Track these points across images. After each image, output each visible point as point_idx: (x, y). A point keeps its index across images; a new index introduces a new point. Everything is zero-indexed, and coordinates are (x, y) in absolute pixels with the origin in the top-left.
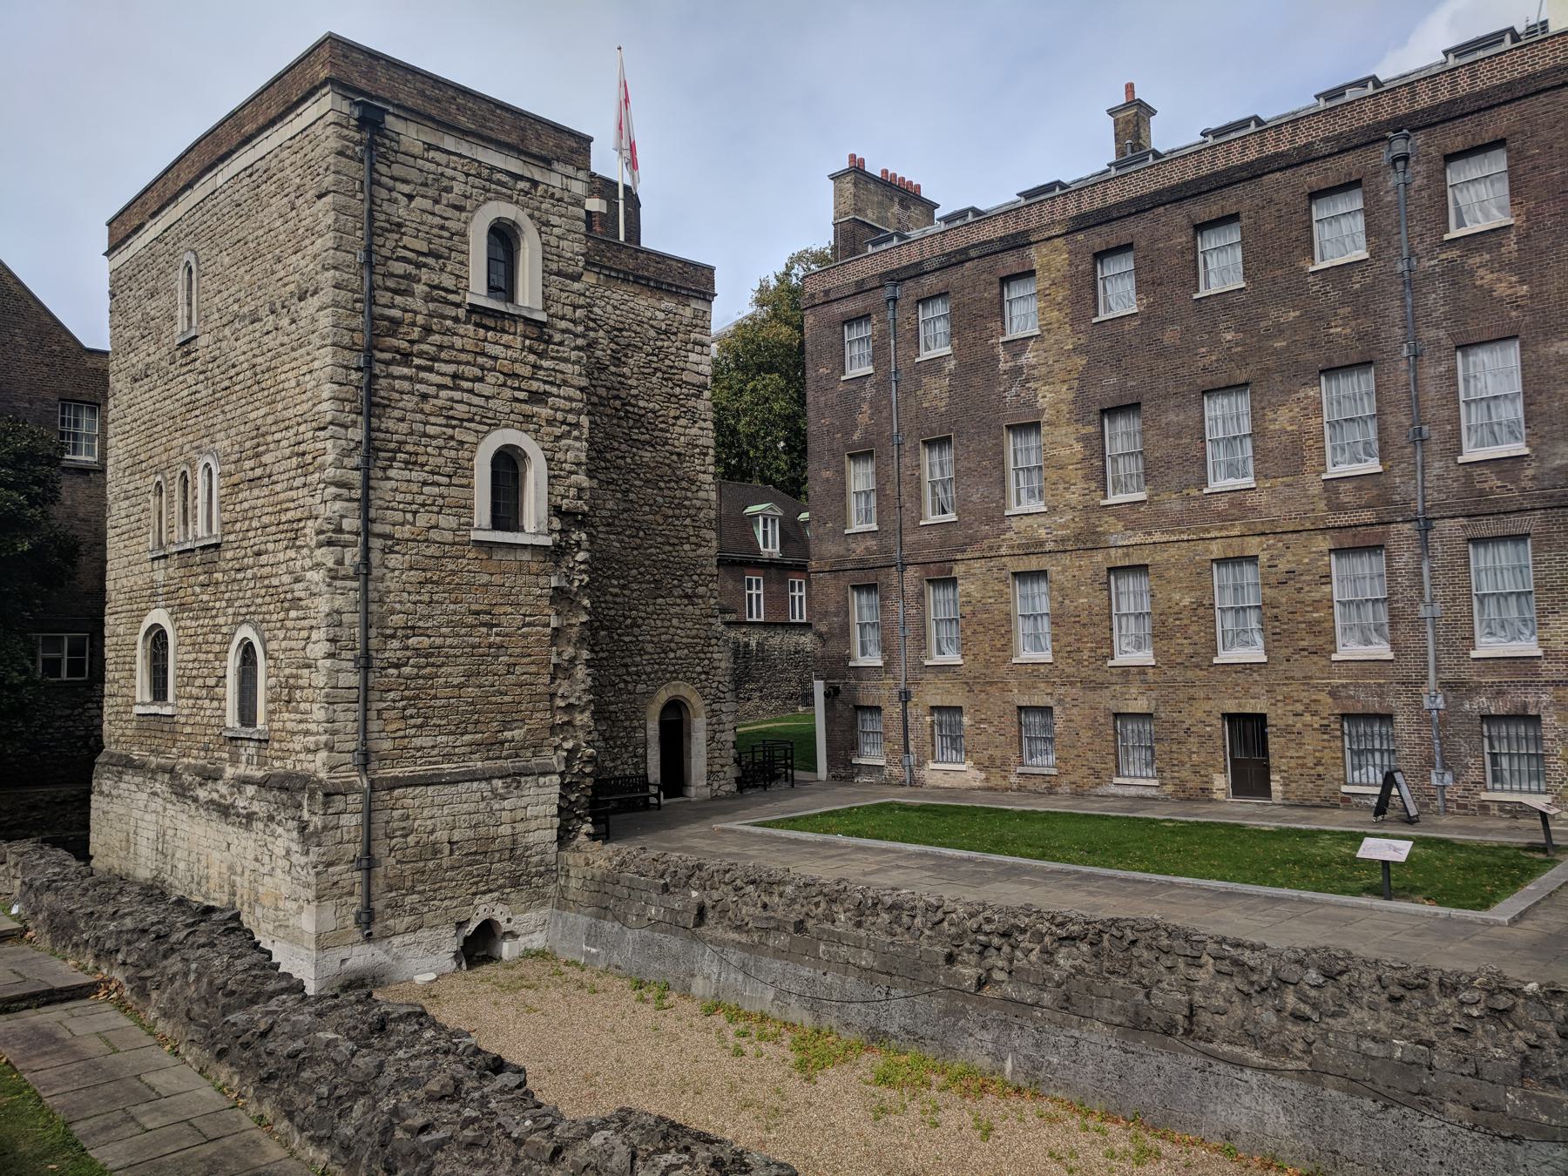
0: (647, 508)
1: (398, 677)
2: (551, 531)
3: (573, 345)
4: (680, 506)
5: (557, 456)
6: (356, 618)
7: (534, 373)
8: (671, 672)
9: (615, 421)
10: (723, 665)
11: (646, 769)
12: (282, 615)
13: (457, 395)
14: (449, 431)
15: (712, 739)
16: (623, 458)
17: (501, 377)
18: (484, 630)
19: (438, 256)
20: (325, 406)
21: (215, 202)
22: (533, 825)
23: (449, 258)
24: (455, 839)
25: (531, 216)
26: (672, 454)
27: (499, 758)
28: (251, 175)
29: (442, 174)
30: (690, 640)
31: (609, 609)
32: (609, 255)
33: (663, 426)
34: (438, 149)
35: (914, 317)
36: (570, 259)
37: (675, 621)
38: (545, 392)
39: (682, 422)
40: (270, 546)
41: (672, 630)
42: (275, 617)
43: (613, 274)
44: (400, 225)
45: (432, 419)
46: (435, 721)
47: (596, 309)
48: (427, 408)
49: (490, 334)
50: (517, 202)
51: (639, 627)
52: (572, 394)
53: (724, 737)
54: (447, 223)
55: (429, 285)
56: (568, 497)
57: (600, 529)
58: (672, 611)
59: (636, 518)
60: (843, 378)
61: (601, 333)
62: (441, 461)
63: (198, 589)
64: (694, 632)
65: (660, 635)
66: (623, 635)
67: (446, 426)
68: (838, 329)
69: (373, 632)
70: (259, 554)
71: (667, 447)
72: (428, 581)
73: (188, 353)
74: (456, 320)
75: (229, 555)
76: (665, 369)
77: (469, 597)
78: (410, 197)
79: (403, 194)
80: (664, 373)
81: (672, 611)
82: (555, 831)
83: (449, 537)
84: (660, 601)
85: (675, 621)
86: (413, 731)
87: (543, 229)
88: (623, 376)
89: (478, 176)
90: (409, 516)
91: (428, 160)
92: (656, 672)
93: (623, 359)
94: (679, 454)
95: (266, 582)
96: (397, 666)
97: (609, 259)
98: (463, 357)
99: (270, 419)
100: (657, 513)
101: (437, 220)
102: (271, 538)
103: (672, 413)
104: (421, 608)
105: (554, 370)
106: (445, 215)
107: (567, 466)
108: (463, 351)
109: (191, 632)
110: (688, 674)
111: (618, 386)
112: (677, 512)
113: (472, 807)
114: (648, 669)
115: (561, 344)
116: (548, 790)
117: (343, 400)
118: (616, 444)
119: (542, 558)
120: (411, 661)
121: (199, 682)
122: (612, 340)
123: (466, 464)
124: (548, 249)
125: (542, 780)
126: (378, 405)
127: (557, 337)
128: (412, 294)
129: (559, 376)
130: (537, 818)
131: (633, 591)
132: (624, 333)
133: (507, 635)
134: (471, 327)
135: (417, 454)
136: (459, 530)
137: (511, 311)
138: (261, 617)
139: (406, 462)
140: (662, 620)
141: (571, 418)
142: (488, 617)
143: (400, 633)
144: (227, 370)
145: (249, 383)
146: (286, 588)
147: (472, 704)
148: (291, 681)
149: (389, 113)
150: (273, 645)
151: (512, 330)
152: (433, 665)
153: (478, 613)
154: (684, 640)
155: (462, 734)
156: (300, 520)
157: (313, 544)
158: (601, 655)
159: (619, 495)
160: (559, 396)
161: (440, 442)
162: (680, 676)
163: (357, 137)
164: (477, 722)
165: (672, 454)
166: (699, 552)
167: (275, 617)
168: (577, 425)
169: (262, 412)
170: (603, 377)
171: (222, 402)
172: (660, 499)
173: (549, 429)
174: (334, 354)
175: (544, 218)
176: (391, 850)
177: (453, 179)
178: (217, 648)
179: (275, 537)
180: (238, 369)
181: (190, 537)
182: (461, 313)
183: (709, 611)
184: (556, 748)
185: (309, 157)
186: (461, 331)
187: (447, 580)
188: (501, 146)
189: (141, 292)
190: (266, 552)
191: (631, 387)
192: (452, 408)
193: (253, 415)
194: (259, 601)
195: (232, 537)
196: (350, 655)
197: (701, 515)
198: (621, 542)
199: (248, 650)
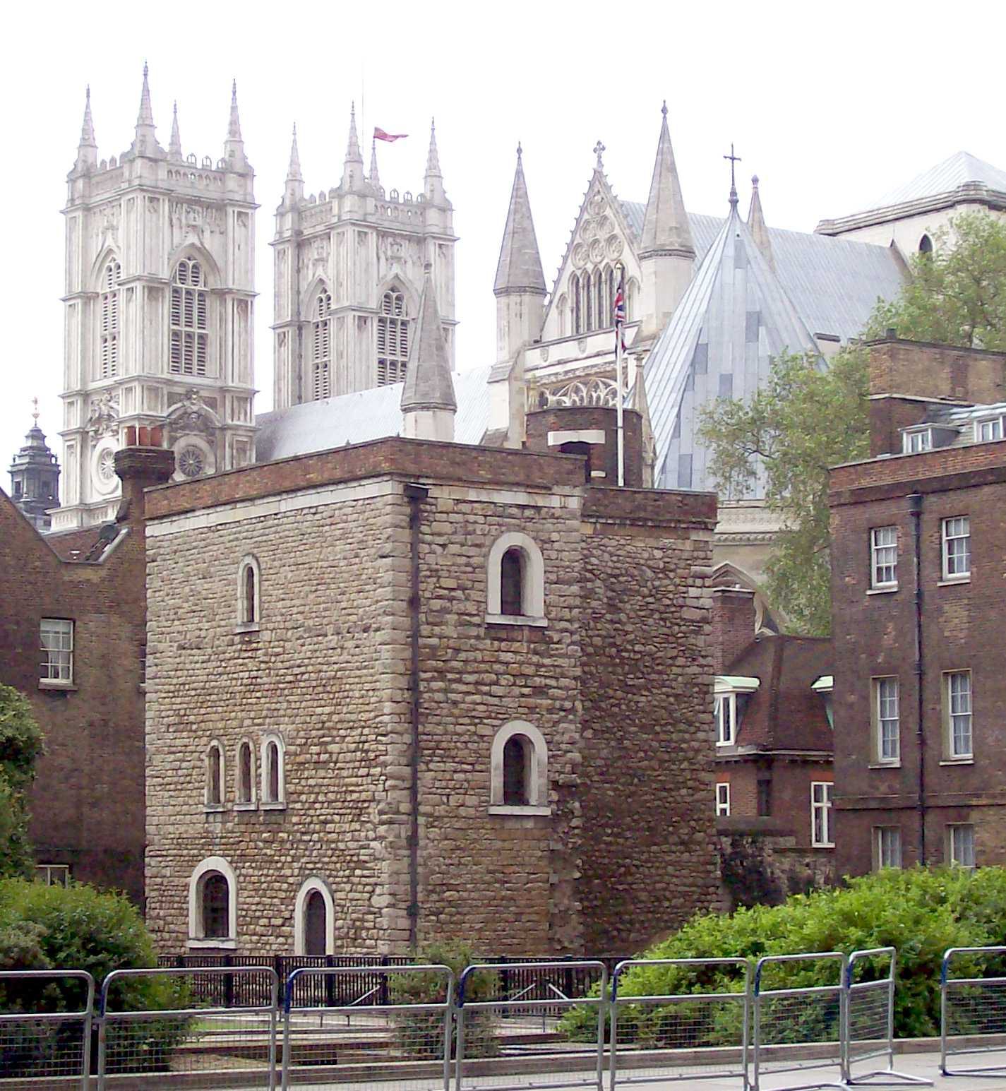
1: (438, 921)
3: (569, 641)
5: (556, 738)
6: (407, 878)
7: (537, 671)
9: (610, 669)
12: (347, 872)
14: (472, 728)
16: (618, 705)
17: (511, 678)
19: (464, 589)
20: (386, 719)
21: (276, 521)
23: (472, 588)
25: (534, 539)
26: (668, 696)
28: (314, 514)
29: (467, 521)
30: (687, 889)
32: (606, 502)
33: (660, 668)
34: (465, 502)
35: (937, 535)
36: (568, 567)
37: (670, 869)
39: (681, 661)
40: (337, 818)
42: (341, 873)
44: (437, 571)
45: (461, 721)
47: (594, 560)
48: (456, 712)
49: (503, 644)
50: (523, 529)
51: (631, 874)
55: (458, 614)
56: (562, 773)
57: (596, 778)
58: (668, 858)
59: (631, 764)
60: (869, 592)
62: (467, 751)
63: (261, 844)
65: (656, 882)
68: (865, 536)
69: (420, 888)
70: (325, 822)
72: (458, 848)
73: (250, 642)
74: (478, 637)
75: (295, 819)
76: (662, 608)
78: (444, 546)
80: (661, 613)
81: (668, 858)
83: (472, 811)
84: (654, 848)
87: (546, 546)
90: (445, 799)
92: (648, 920)
93: (620, 605)
94: (676, 696)
95: (333, 846)
96: (437, 914)
97: (606, 506)
99: (335, 718)
102: (336, 811)
105: (553, 666)
107: (563, 746)
108: (483, 662)
109: (254, 879)
111: (613, 633)
112: (673, 755)
117: (399, 714)
118: (611, 692)
120: (447, 910)
121: (263, 921)
123: (483, 752)
126: (422, 714)
127: (556, 638)
128: (446, 624)
129: (558, 670)
132: (622, 579)
134: (488, 642)
138: (328, 872)
139: (441, 756)
140: (658, 868)
141: (568, 705)
143: (438, 889)
144: (291, 667)
145: (314, 683)
146: (352, 852)
148: (358, 923)
150: (339, 895)
154: (680, 889)
156: (364, 801)
157: (376, 821)
158: (595, 903)
159: (613, 743)
161: (466, 738)
163: (408, 510)
166: (696, 797)
167: (341, 873)
168: (572, 710)
169: (327, 710)
171: (286, 692)
172: (655, 744)
174: (394, 679)
175: (545, 536)
177: (476, 522)
178: (283, 895)
179: (341, 811)
180: (303, 669)
181: (253, 799)
182: (482, 631)
185: (371, 521)
186: (481, 647)
189: (189, 569)
190: (332, 822)
191: (627, 633)
193: (319, 710)
194: (326, 859)
195: (298, 806)
196: (403, 905)
197: (700, 757)
198: (615, 790)
199: (315, 899)
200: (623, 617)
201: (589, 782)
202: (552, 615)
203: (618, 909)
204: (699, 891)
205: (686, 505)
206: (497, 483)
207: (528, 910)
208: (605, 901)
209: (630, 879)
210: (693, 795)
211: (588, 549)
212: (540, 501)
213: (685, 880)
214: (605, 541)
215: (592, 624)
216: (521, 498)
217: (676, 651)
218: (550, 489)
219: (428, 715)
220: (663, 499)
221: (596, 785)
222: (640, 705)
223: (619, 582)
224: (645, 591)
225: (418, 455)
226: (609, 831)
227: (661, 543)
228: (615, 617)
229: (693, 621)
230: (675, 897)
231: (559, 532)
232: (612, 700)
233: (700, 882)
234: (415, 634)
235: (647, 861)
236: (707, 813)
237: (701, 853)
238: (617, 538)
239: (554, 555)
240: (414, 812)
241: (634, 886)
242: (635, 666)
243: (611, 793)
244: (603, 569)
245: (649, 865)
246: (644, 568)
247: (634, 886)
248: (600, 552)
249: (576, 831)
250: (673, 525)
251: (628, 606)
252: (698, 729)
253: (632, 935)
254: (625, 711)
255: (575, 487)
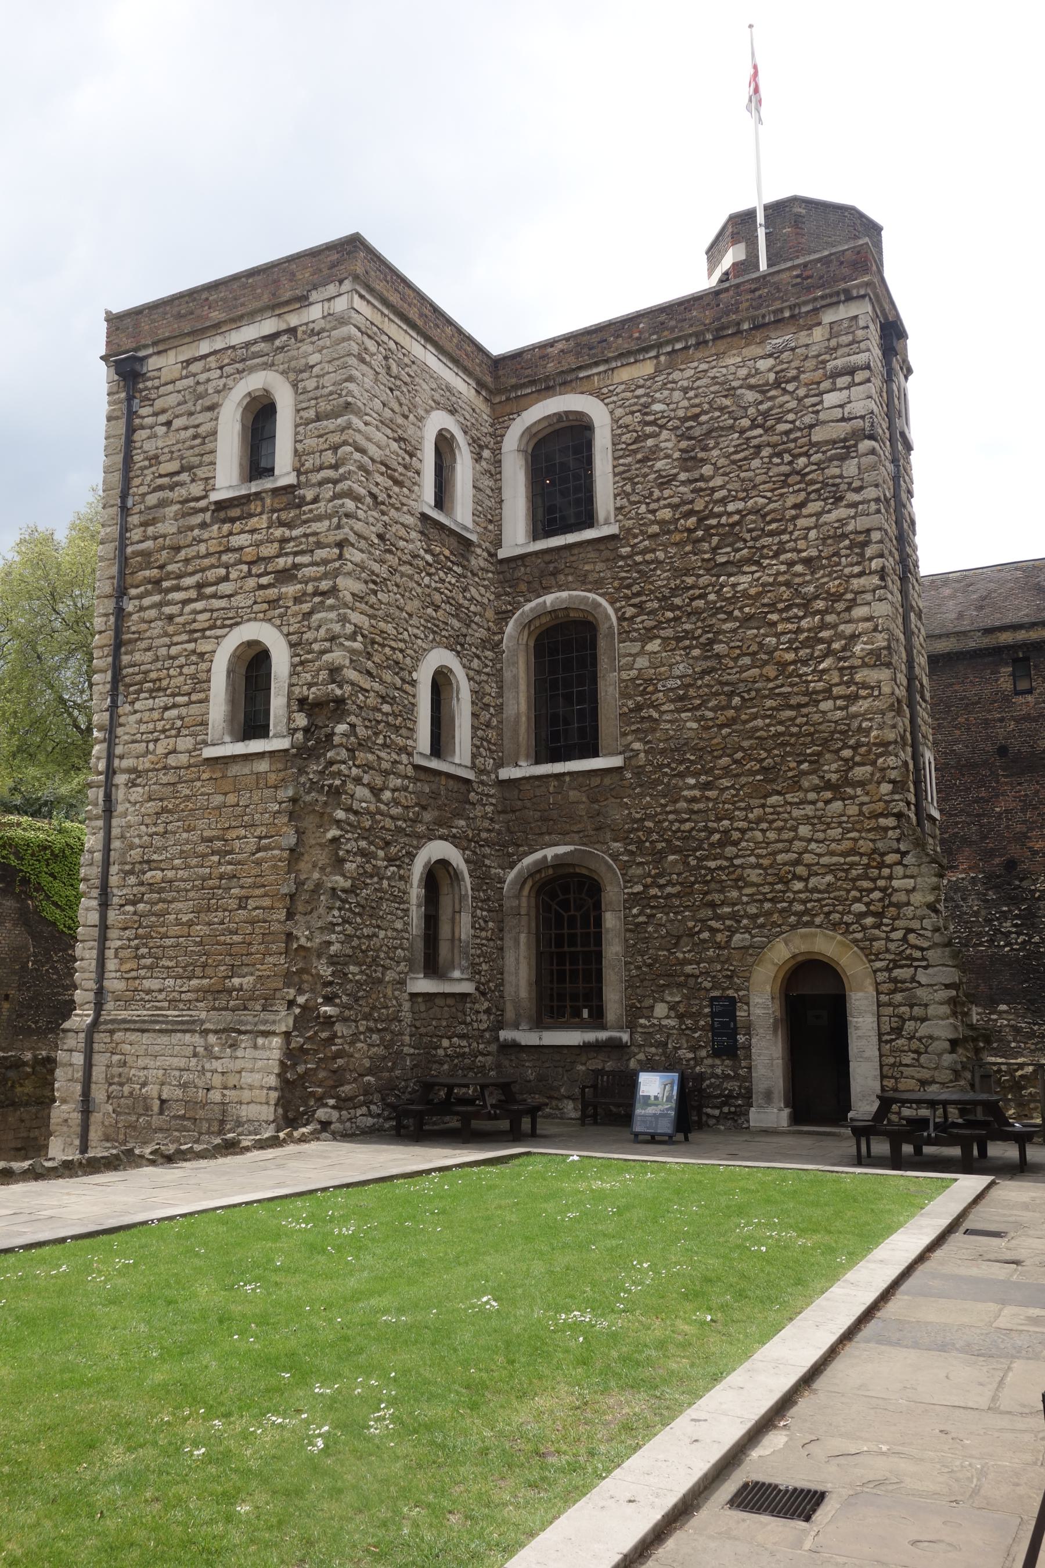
0: (747, 660)
1: (135, 913)
2: (293, 732)
4: (813, 641)
7: (282, 548)
8: (800, 914)
9: (688, 548)
10: (917, 898)
11: (750, 1068)
13: (199, 605)
14: (191, 646)
15: (898, 1031)
17: (245, 568)
18: (216, 858)
22: (246, 1095)
23: (200, 465)
24: (164, 1097)
27: (226, 1009)
29: (198, 383)
30: (835, 859)
31: (683, 821)
32: (673, 323)
33: (774, 526)
36: (331, 393)
37: (804, 830)
38: (296, 566)
39: (814, 507)
41: (798, 845)
43: (678, 346)
44: (156, 457)
45: (175, 639)
46: (165, 962)
47: (657, 407)
48: (171, 629)
50: (273, 365)
51: (735, 844)
52: (324, 556)
53: (924, 1030)
54: (200, 430)
55: (179, 502)
56: (316, 684)
57: (665, 708)
58: (796, 813)
59: (726, 678)
61: (665, 435)
62: (182, 678)
64: (846, 845)
65: (774, 854)
66: (706, 858)
67: (189, 641)
69: (114, 869)
71: (782, 557)
72: (164, 810)
74: (203, 525)
76: (776, 438)
77: (201, 824)
79: (162, 425)
81: (796, 813)
82: (272, 1109)
83: (184, 759)
84: (774, 799)
85: (804, 830)
86: (142, 972)
88: (702, 478)
89: (234, 361)
90: (151, 746)
91: (187, 377)
92: (768, 914)
94: (807, 562)
96: (134, 903)
98: (206, 562)
100: (766, 663)
101: (191, 432)
103: (791, 500)
104: (158, 841)
105: (306, 535)
106: (197, 422)
107: (316, 647)
108: (208, 555)
110: (836, 917)
111: (691, 496)
112: (803, 653)
113: (182, 1063)
114: (752, 910)
115: (316, 500)
116: (267, 1054)
118: (690, 580)
119: (280, 766)
122: (682, 437)
123: (203, 676)
124: (302, 397)
125: (260, 1041)
126: (130, 641)
127: (309, 494)
129: (311, 539)
130: (251, 1087)
131: (723, 790)
132: (704, 418)
133: (239, 863)
135: (160, 680)
136: (195, 750)
137: (253, 490)
139: (151, 691)
140: (780, 830)
141: (325, 585)
142: (219, 844)
143: (138, 867)
147: (200, 944)
149: (150, 356)
151: (259, 510)
152: (164, 901)
153: (210, 840)
154: (825, 860)
155: (190, 978)
158: (669, 890)
160: (313, 564)
161: (182, 660)
162: (818, 920)
164: (204, 966)
165: (791, 564)
166: (853, 709)
170: (667, 493)
173: (296, 608)
176: (109, 1097)
177: (209, 380)
183: (879, 807)
184: (291, 1003)
186: (206, 536)
187: (182, 806)
188: (251, 316)
191: (713, 490)
192: (194, 621)
198: (698, 721)
200: (707, 470)
201: (656, 715)
202: (308, 465)
203: (709, 898)
204: (865, 860)
205: (808, 277)
206: (233, 320)
207: (260, 891)
208: (687, 889)
209: (730, 851)
210: (846, 708)
211: (647, 395)
212: (293, 320)
213: (833, 845)
214: (676, 375)
215: (657, 493)
216: (269, 326)
217: (803, 494)
218: (306, 298)
219: (136, 640)
220: (765, 286)
221: (666, 717)
222: (740, 588)
223: (700, 424)
224: (745, 423)
225: (137, 326)
226: (692, 781)
227: (769, 349)
228: (696, 474)
229: (834, 442)
230: (817, 874)
231: (320, 351)
232: (691, 592)
233: (865, 846)
234: (123, 542)
235: (759, 820)
236: (874, 733)
237: (866, 799)
238: (696, 364)
239: (311, 384)
240: (110, 772)
241: (737, 862)
242: (731, 535)
243: (695, 725)
244: (672, 414)
245: (764, 826)
246: (739, 392)
247: (737, 862)
248: (666, 393)
249: (335, 768)
250: (787, 314)
251: (715, 453)
252: (853, 604)
253: (737, 937)
254: (715, 602)
255: (341, 282)
